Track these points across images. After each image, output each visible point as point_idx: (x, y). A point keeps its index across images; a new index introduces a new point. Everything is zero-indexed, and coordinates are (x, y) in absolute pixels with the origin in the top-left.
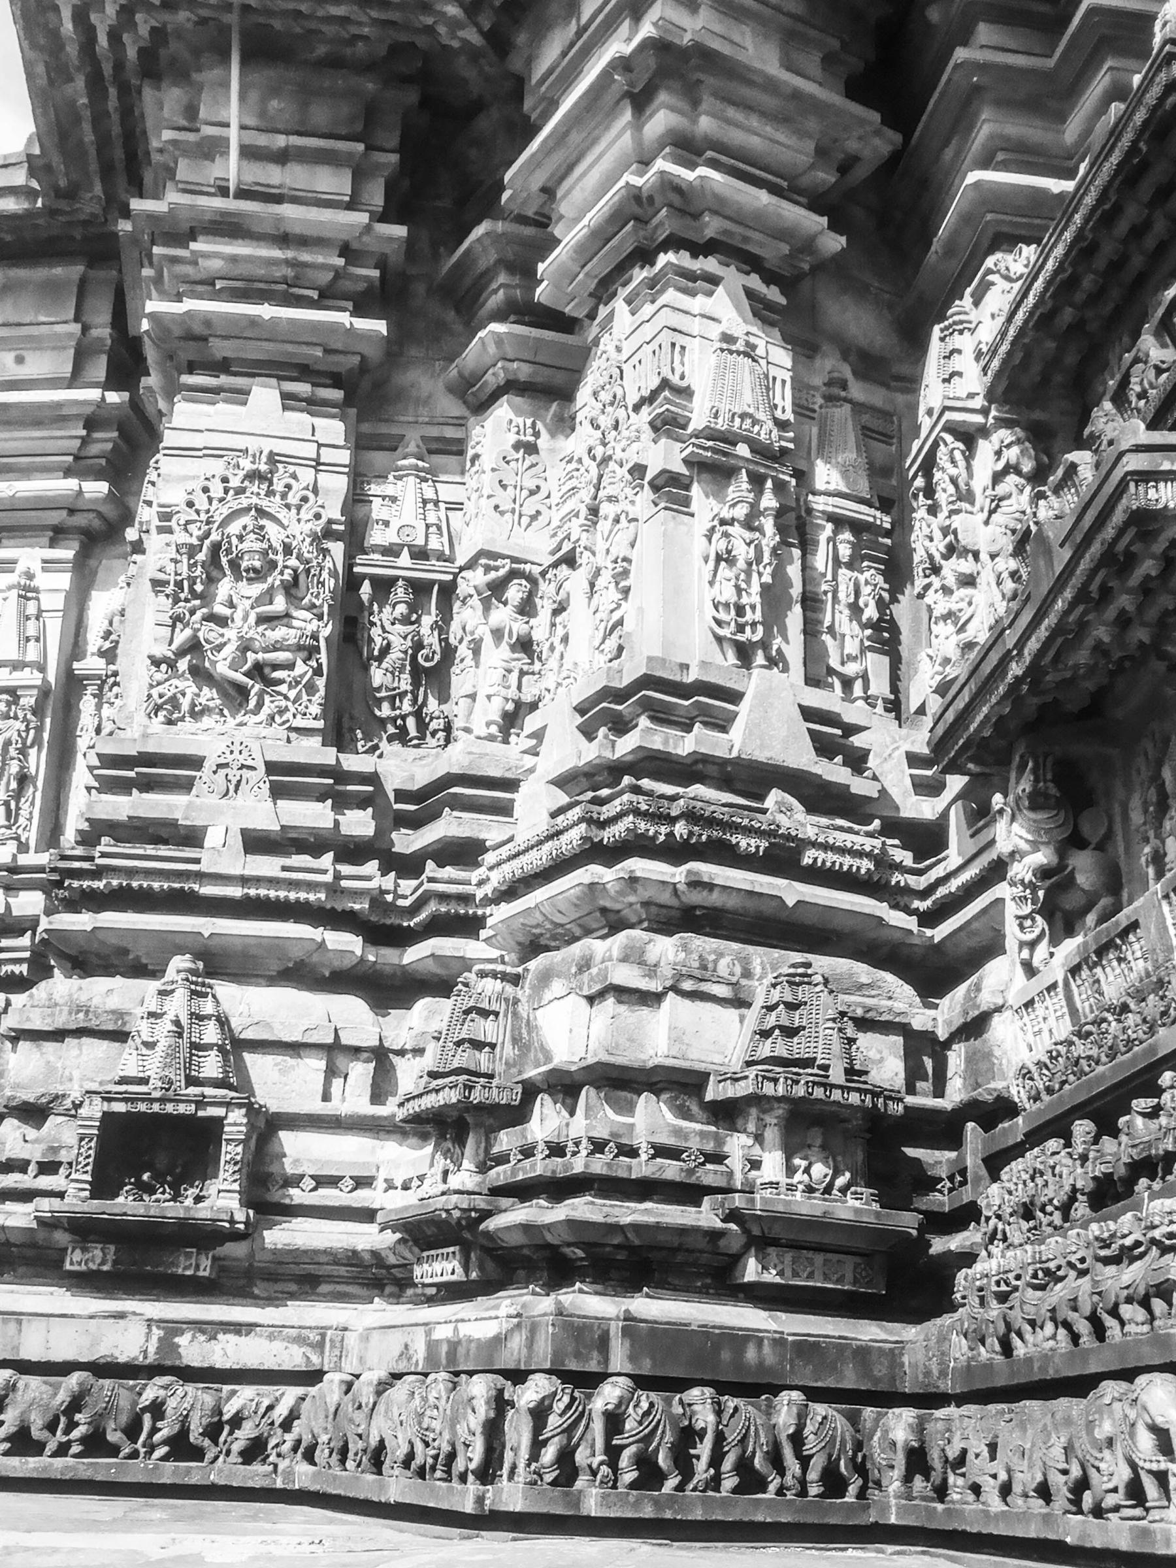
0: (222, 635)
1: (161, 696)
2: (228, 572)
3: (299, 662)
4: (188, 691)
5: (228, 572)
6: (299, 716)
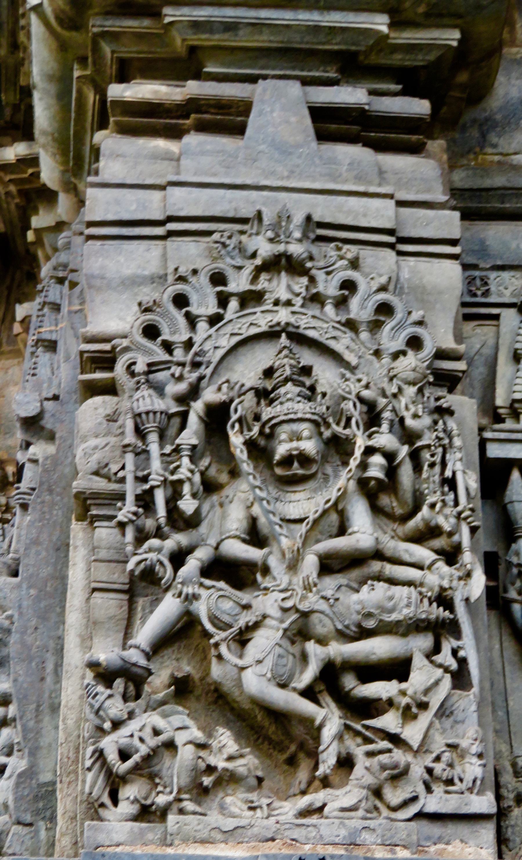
0: (247, 607)
1: (124, 755)
2: (247, 467)
3: (419, 661)
4: (180, 738)
5: (247, 467)
6: (438, 789)
